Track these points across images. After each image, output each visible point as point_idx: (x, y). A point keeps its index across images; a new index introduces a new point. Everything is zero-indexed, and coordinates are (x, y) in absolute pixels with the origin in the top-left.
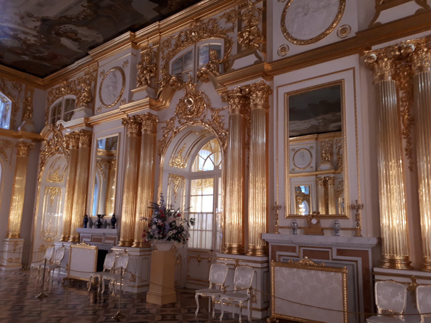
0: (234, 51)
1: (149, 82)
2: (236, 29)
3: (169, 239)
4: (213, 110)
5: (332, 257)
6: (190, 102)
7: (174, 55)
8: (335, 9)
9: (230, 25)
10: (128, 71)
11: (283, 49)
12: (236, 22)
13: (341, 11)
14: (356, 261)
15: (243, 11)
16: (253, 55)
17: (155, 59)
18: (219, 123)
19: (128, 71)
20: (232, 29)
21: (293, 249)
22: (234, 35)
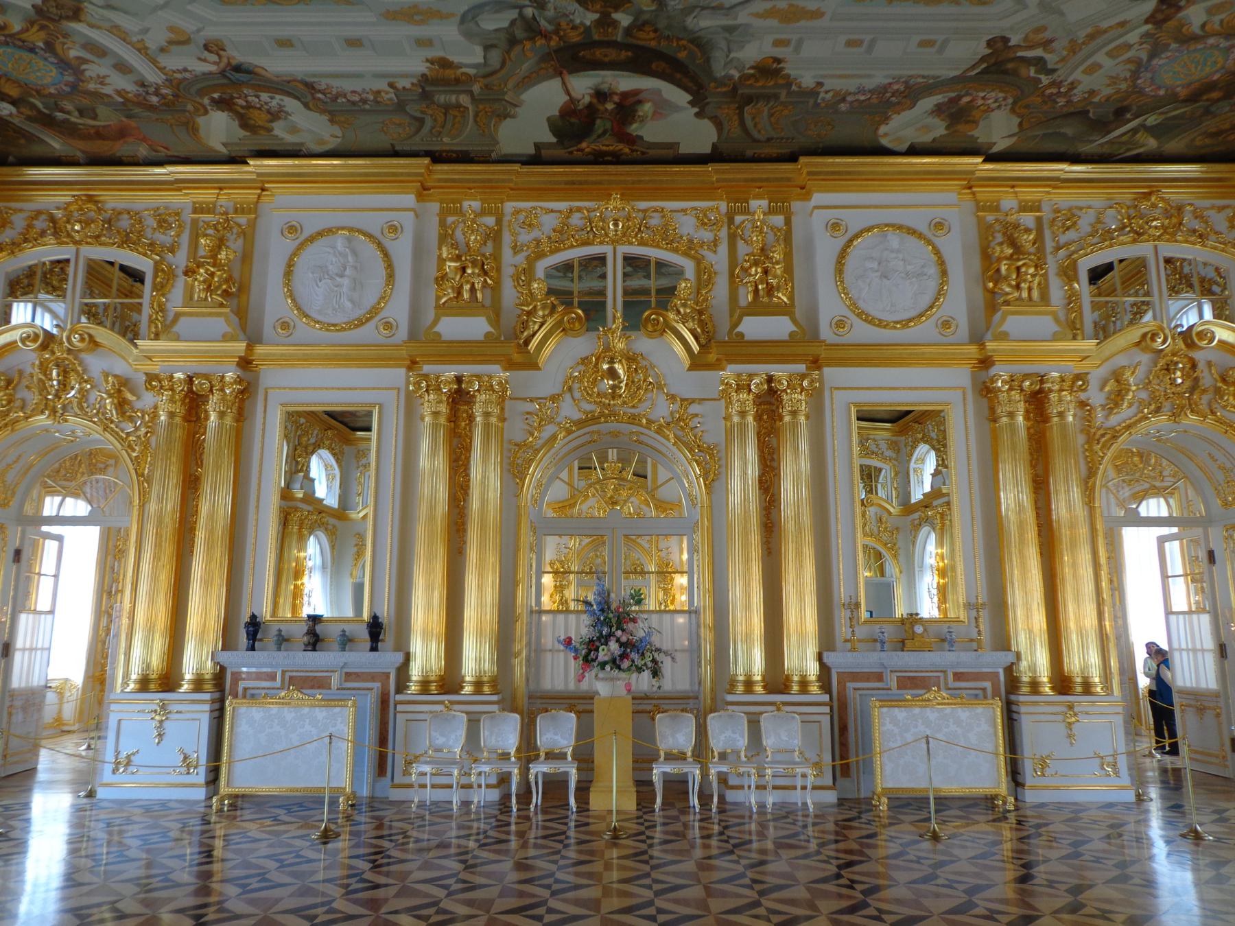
0: (720, 291)
1: (479, 295)
2: (723, 249)
3: (602, 666)
4: (672, 398)
5: (946, 684)
6: (612, 373)
7: (552, 252)
8: (932, 285)
9: (707, 235)
10: (402, 250)
11: (840, 324)
12: (724, 233)
13: (940, 293)
14: (984, 690)
15: (738, 219)
16: (786, 319)
17: (490, 244)
18: (692, 429)
19: (402, 250)
20: (715, 243)
21: (879, 677)
22: (719, 259)
